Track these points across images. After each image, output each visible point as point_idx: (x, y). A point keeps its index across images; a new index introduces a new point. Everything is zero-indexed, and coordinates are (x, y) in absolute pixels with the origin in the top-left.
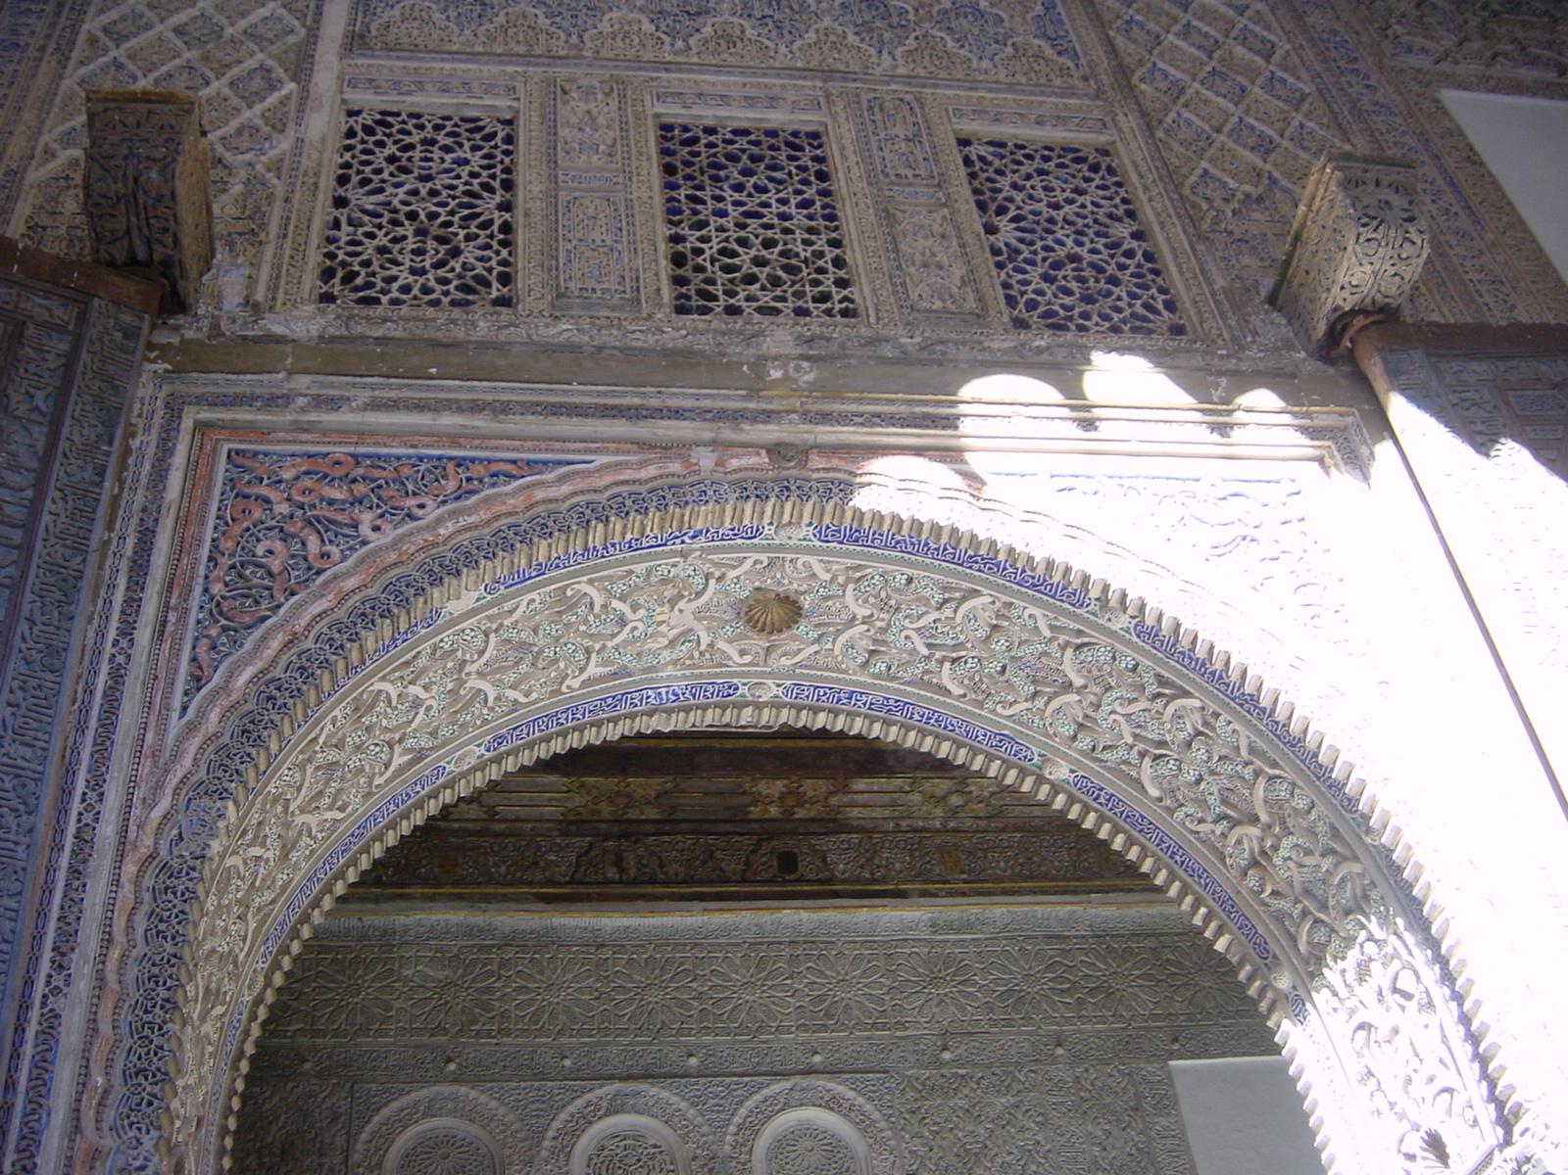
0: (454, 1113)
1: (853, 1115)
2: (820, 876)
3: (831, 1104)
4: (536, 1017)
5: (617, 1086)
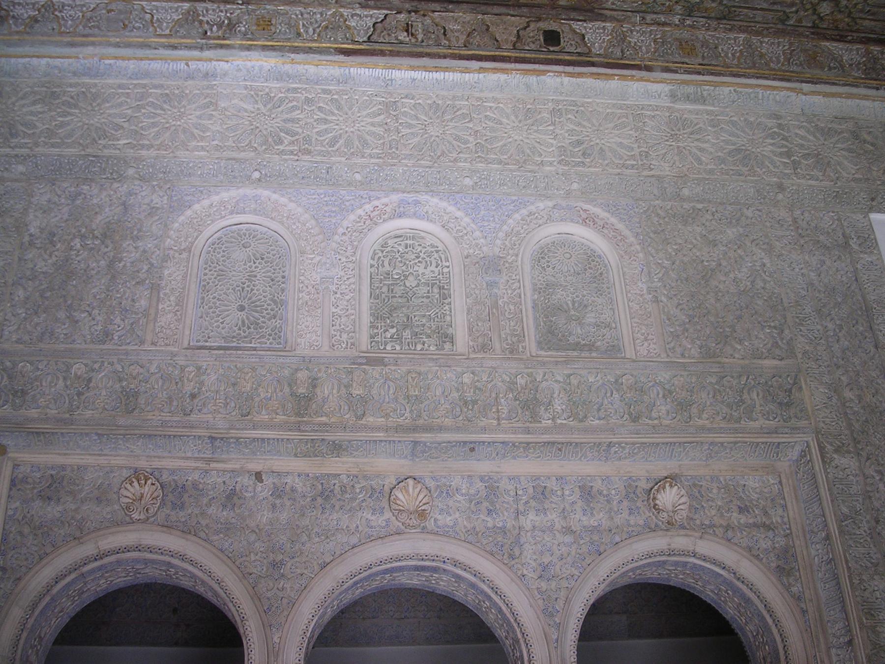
0: (255, 212)
1: (606, 231)
2: (579, 50)
3: (588, 220)
4: (333, 142)
5: (401, 196)
